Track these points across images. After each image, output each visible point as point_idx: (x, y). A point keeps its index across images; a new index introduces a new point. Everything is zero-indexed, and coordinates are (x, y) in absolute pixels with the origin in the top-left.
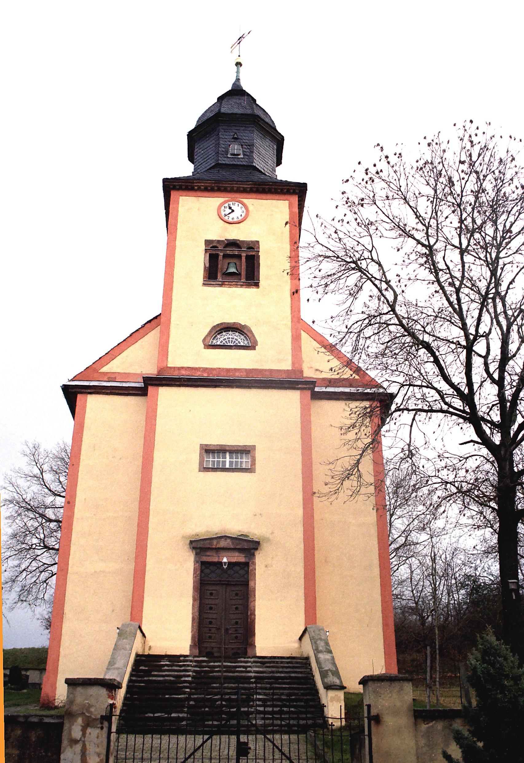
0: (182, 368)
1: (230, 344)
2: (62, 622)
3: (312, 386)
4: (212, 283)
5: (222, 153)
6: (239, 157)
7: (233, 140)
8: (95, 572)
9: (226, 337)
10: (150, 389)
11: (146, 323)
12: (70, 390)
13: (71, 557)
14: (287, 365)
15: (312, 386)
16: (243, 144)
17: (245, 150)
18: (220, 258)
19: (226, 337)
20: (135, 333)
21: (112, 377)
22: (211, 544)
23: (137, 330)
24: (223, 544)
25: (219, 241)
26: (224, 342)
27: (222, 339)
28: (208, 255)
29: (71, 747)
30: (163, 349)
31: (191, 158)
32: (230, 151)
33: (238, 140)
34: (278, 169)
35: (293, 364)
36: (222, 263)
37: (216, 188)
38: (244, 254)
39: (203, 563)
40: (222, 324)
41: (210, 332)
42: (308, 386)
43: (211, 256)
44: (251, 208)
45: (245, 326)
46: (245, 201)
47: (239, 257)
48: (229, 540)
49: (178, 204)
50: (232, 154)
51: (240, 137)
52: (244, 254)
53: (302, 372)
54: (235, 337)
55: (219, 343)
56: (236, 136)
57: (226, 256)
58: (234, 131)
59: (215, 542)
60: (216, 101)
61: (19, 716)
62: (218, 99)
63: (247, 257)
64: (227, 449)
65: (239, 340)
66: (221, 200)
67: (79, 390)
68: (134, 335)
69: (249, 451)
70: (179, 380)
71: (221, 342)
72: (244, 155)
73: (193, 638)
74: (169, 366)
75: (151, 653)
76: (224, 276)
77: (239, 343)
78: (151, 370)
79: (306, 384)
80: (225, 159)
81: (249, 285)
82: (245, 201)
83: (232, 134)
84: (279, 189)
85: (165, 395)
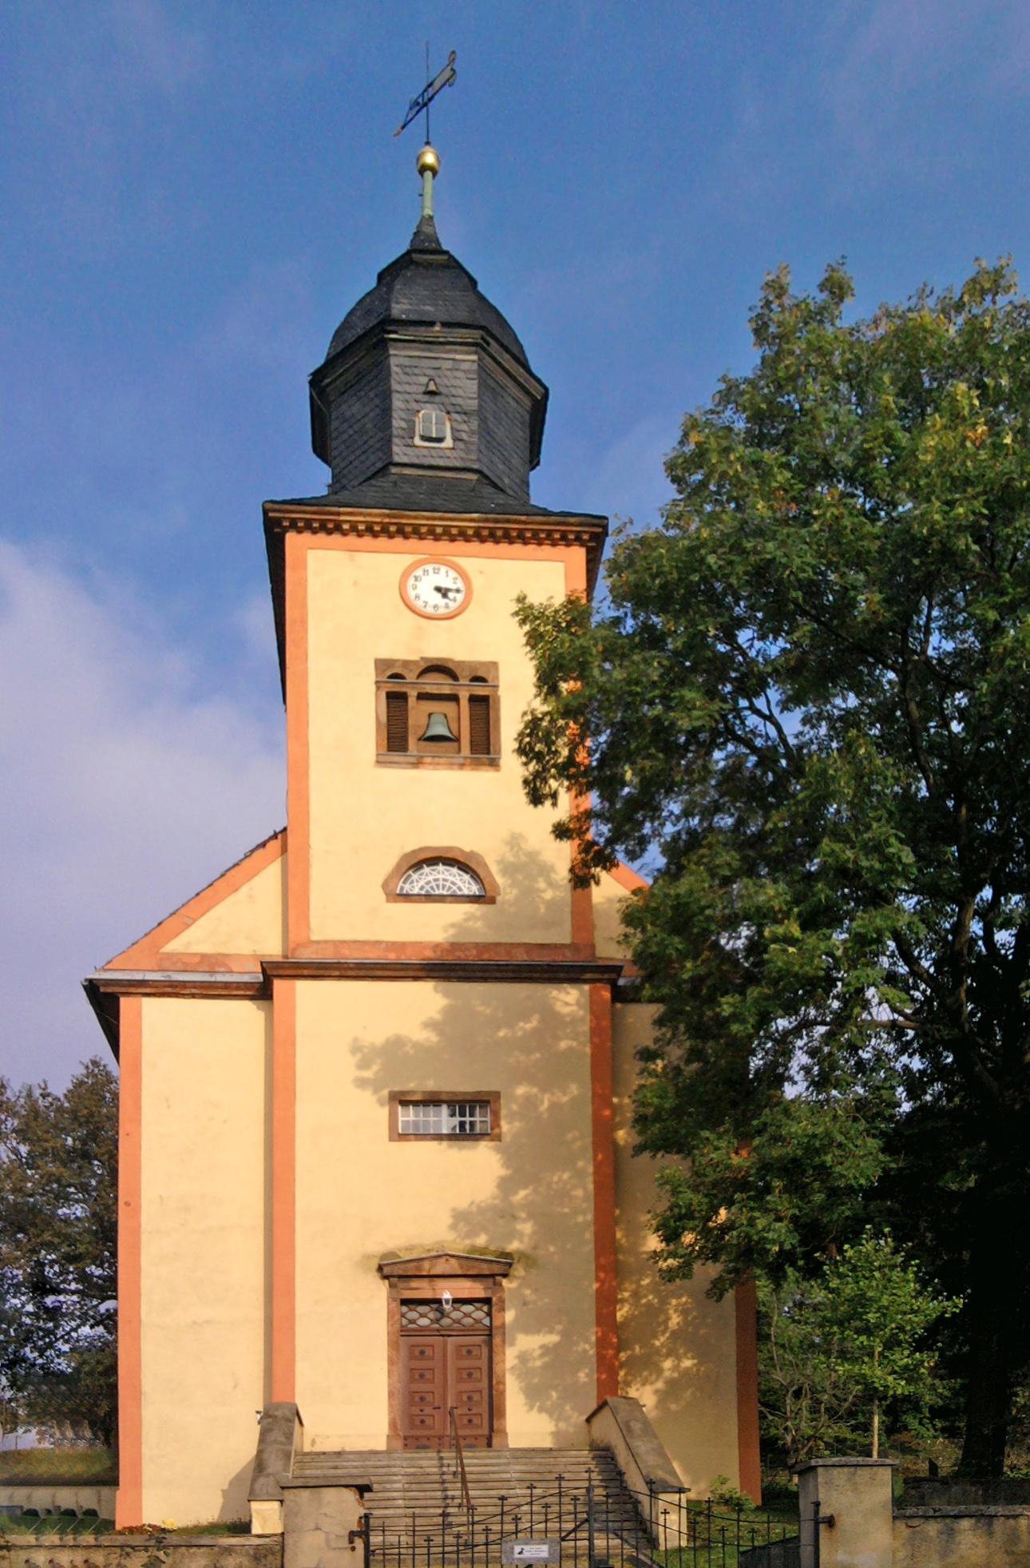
0: (343, 942)
1: (441, 892)
2: (139, 1406)
3: (613, 976)
4: (397, 759)
5: (401, 432)
6: (442, 445)
7: (426, 398)
8: (195, 1323)
9: (430, 878)
10: (278, 985)
11: (252, 851)
12: (102, 990)
13: (143, 1299)
14: (562, 935)
15: (613, 976)
16: (451, 408)
17: (455, 425)
18: (412, 701)
19: (430, 878)
20: (233, 872)
21: (184, 962)
22: (419, 1268)
23: (237, 865)
24: (441, 1267)
25: (406, 663)
26: (427, 887)
27: (422, 883)
28: (383, 696)
29: (552, 1433)
30: (294, 900)
31: (321, 448)
32: (419, 429)
33: (437, 399)
34: (532, 473)
35: (576, 929)
36: (417, 713)
37: (393, 529)
38: (464, 696)
39: (405, 1302)
40: (421, 850)
41: (398, 866)
42: (606, 976)
43: (391, 696)
44: (477, 582)
45: (472, 854)
46: (463, 562)
47: (454, 698)
48: (453, 1261)
49: (305, 568)
50: (424, 438)
51: (442, 389)
52: (464, 696)
53: (593, 946)
54: (451, 878)
55: (416, 891)
56: (432, 387)
57: (422, 697)
58: (429, 372)
59: (426, 1265)
60: (373, 284)
61: (598, 1379)
62: (381, 276)
63: (473, 699)
64: (444, 1098)
65: (460, 884)
66: (407, 560)
67: (123, 990)
68: (229, 874)
69: (488, 1102)
70: (338, 966)
71: (422, 888)
72: (455, 439)
73: (393, 1425)
74: (314, 937)
75: (317, 1449)
76: (423, 744)
77: (460, 889)
78: (273, 948)
79: (603, 972)
80: (409, 450)
81: (476, 764)
82: (463, 562)
83: (424, 380)
84: (543, 531)
85: (307, 998)
